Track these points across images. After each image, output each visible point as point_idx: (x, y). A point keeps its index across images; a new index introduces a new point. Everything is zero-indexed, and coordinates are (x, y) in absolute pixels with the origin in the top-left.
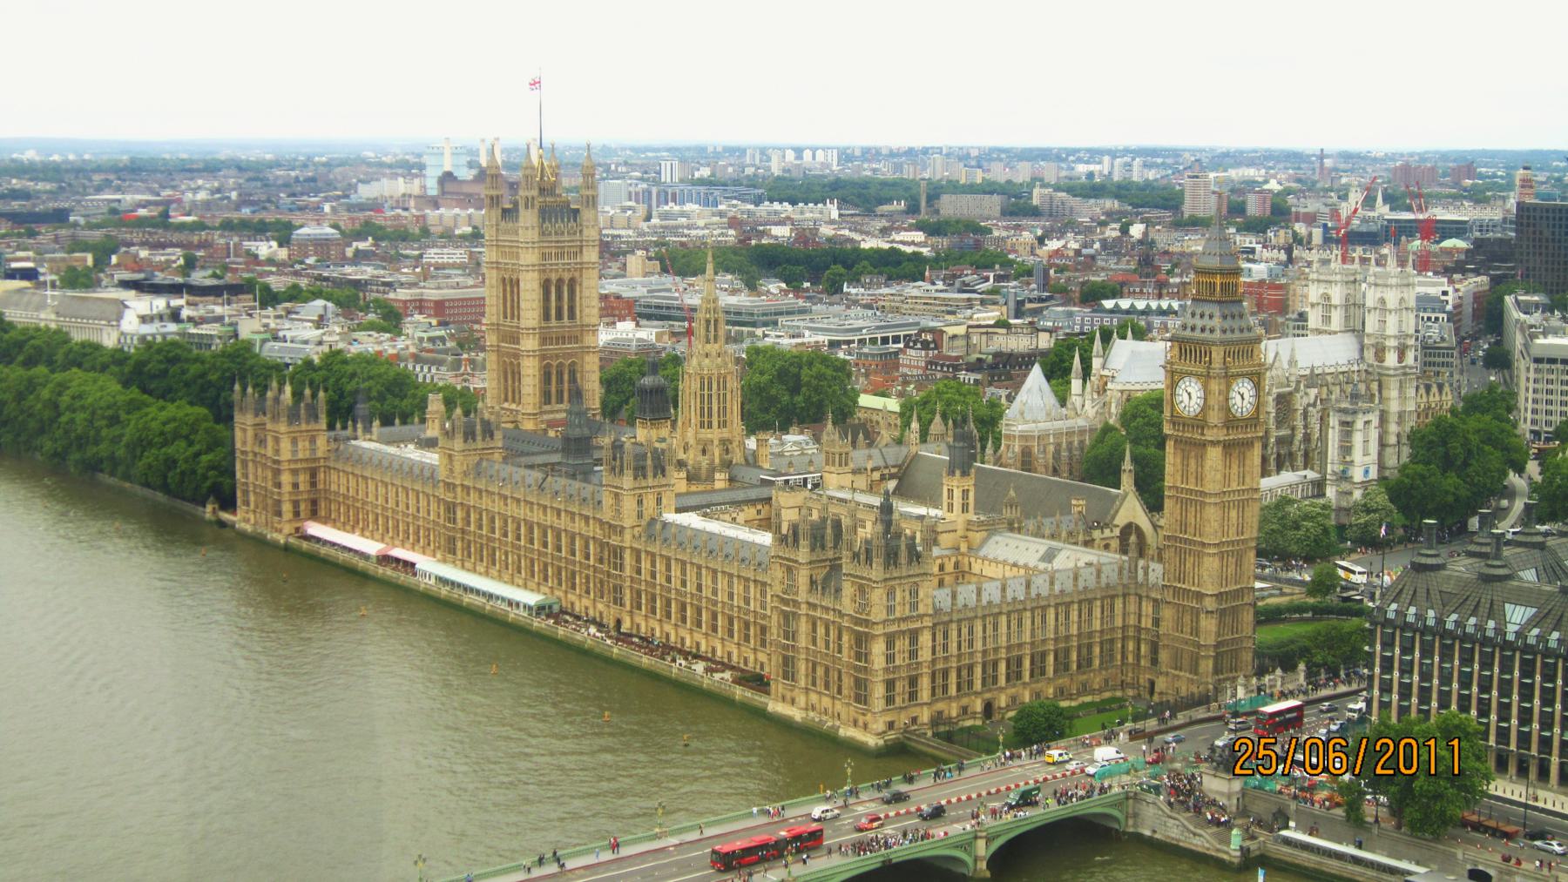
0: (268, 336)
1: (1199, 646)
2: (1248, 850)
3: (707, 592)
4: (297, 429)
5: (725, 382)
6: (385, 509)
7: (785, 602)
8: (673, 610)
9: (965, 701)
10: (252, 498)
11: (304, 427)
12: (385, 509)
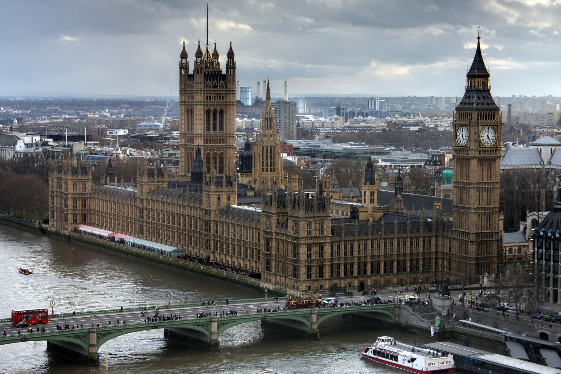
0: (88, 152)
1: (467, 258)
2: (444, 327)
3: (244, 239)
4: (76, 178)
5: (275, 150)
6: (114, 215)
7: (267, 233)
8: (230, 249)
9: (349, 280)
10: (55, 215)
11: (80, 177)
12: (114, 215)
